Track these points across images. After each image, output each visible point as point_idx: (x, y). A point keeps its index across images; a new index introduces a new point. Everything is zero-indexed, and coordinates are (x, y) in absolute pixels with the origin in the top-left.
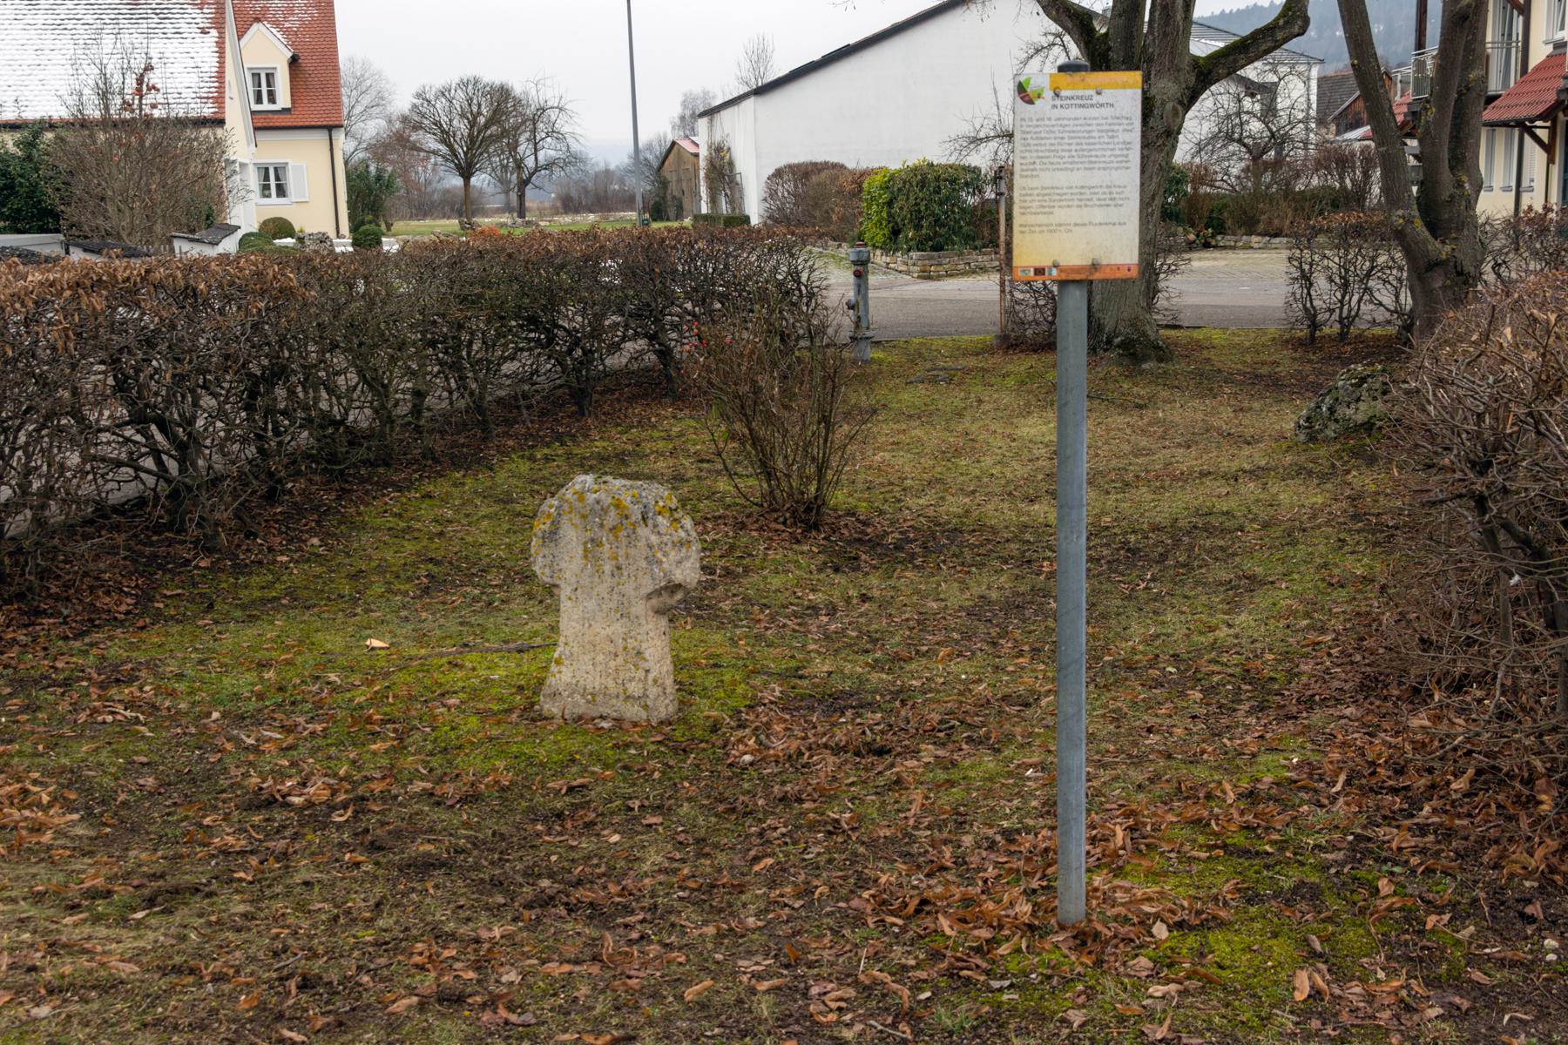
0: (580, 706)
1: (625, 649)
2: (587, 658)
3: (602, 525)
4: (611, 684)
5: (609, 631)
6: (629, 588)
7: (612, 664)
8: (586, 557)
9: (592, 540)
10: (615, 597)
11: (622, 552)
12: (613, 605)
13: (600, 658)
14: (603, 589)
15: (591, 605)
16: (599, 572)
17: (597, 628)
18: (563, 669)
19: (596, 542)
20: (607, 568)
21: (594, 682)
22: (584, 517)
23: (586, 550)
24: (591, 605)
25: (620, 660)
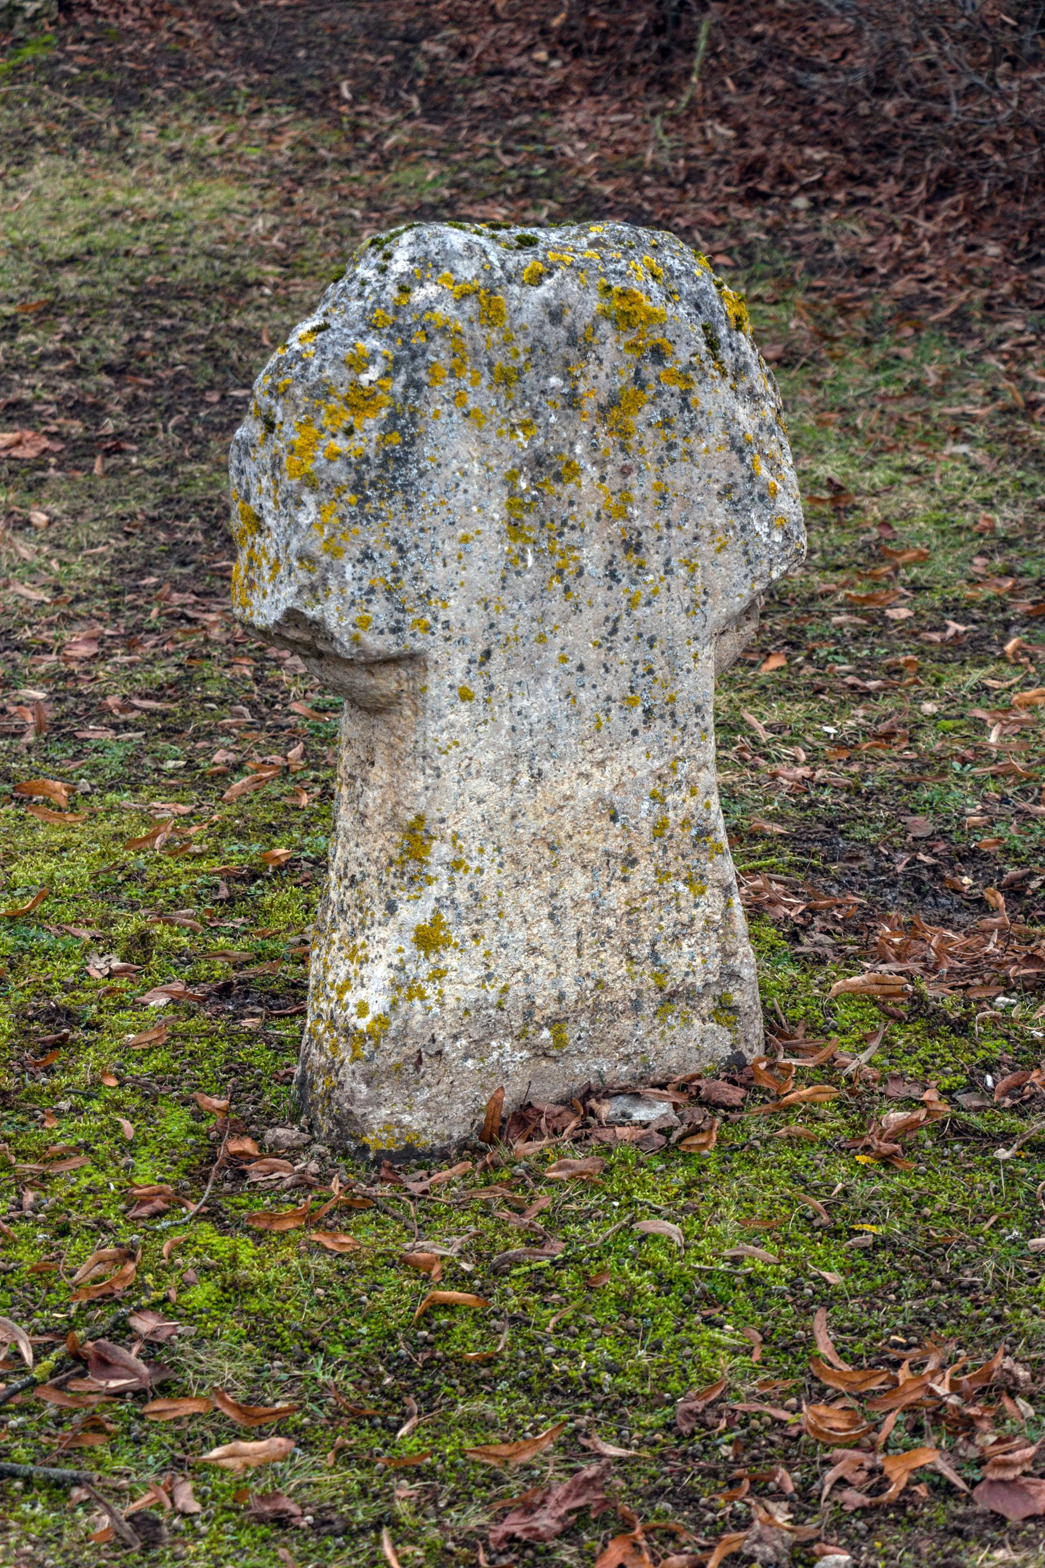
0: (515, 1071)
1: (660, 829)
2: (526, 898)
3: (573, 401)
4: (614, 966)
5: (604, 781)
6: (668, 615)
7: (617, 896)
8: (514, 528)
9: (539, 461)
10: (623, 653)
11: (642, 486)
12: (615, 686)
13: (577, 884)
14: (578, 636)
15: (541, 702)
16: (565, 574)
17: (563, 780)
18: (451, 959)
19: (549, 467)
20: (593, 555)
21: (554, 976)
22: (506, 379)
23: (516, 504)
24: (541, 702)
25: (643, 873)
